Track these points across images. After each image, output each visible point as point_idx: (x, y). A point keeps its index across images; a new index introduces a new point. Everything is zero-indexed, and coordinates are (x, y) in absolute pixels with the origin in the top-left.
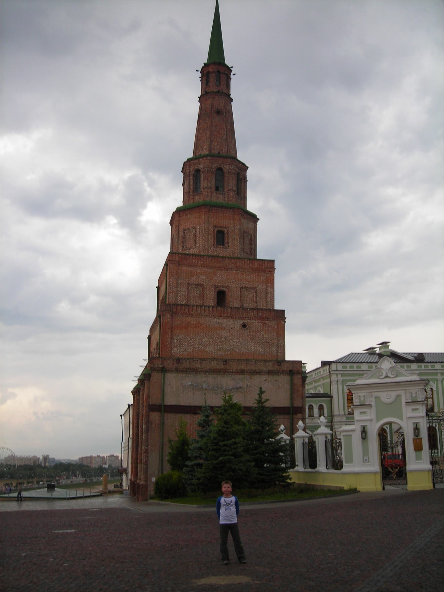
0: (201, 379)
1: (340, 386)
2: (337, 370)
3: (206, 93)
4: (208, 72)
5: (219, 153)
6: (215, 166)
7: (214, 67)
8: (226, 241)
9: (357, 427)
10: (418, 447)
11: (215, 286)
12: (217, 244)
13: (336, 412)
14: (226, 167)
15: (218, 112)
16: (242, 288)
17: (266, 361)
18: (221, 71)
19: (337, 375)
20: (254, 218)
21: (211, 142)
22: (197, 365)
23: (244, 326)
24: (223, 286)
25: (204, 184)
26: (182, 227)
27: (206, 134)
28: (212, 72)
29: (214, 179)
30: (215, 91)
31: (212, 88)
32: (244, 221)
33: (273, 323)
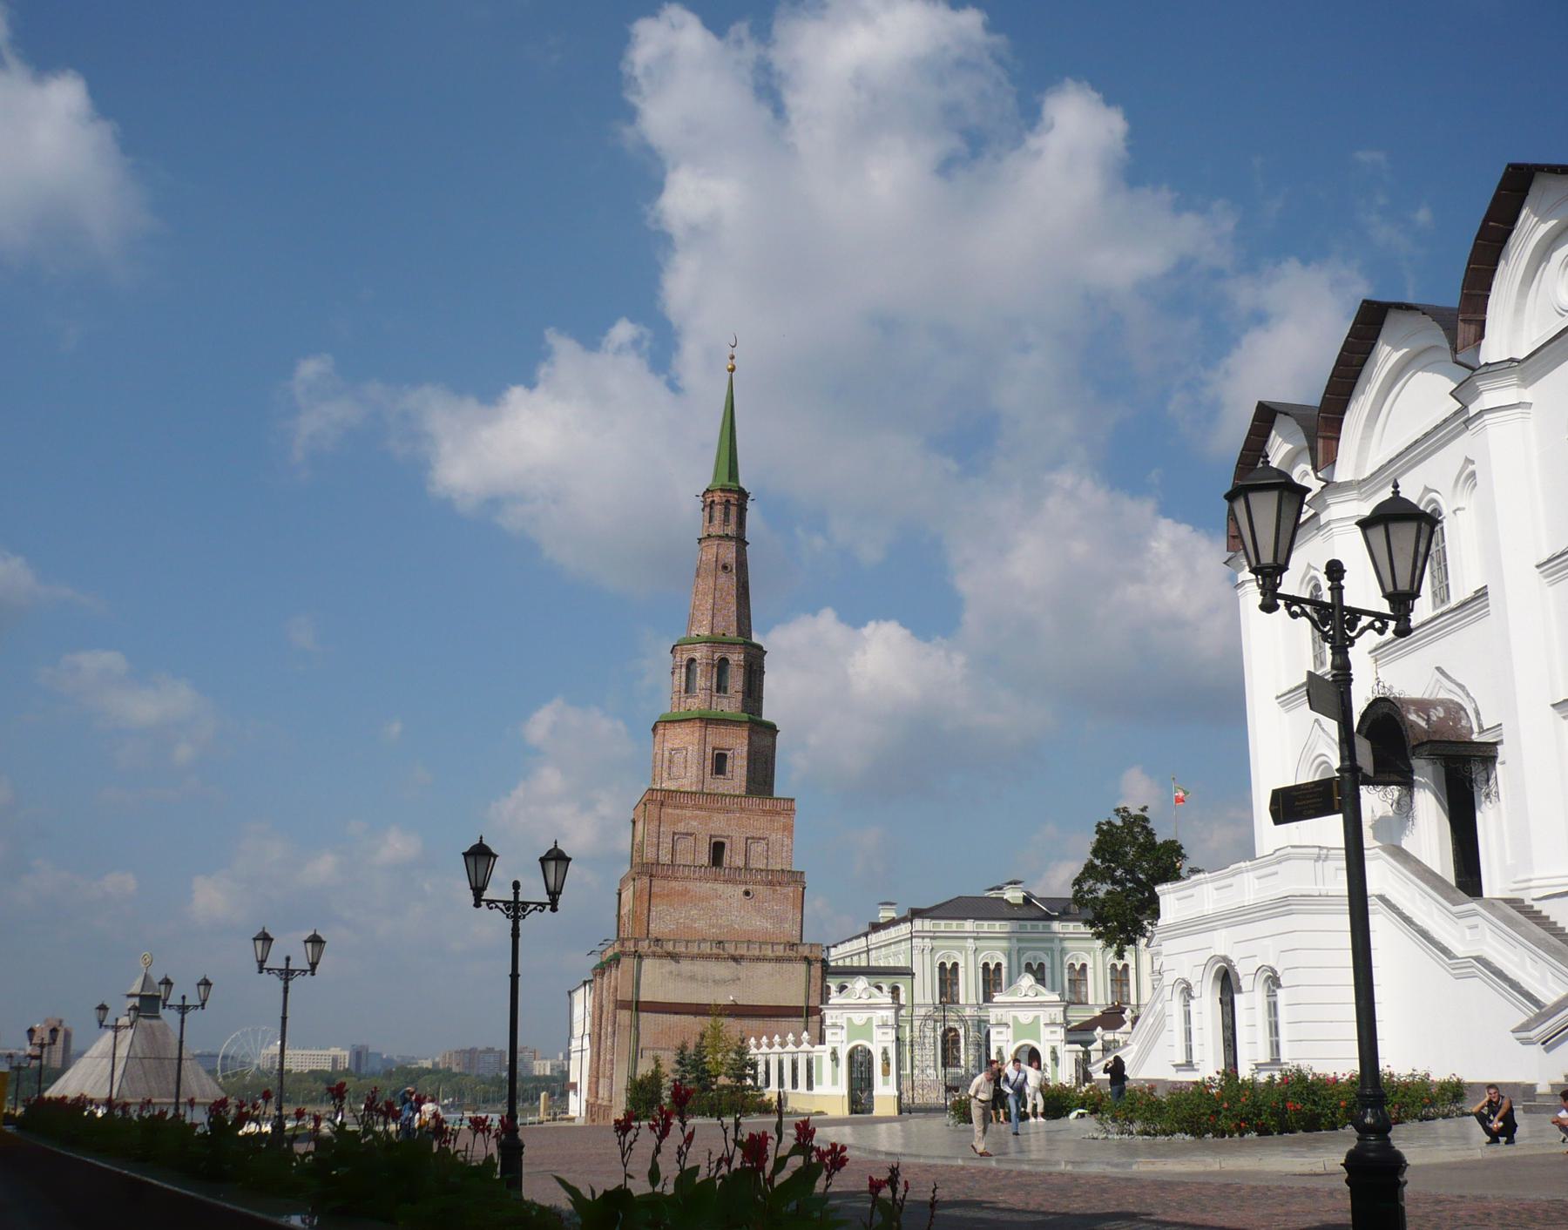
0: (686, 966)
1: (928, 957)
6: (716, 656)
9: (827, 1048)
10: (886, 1073)
13: (916, 1001)
15: (725, 567)
17: (773, 944)
18: (733, 501)
20: (772, 729)
22: (681, 949)
23: (747, 893)
25: (700, 682)
26: (668, 745)
31: (716, 529)
32: (754, 738)
33: (789, 890)
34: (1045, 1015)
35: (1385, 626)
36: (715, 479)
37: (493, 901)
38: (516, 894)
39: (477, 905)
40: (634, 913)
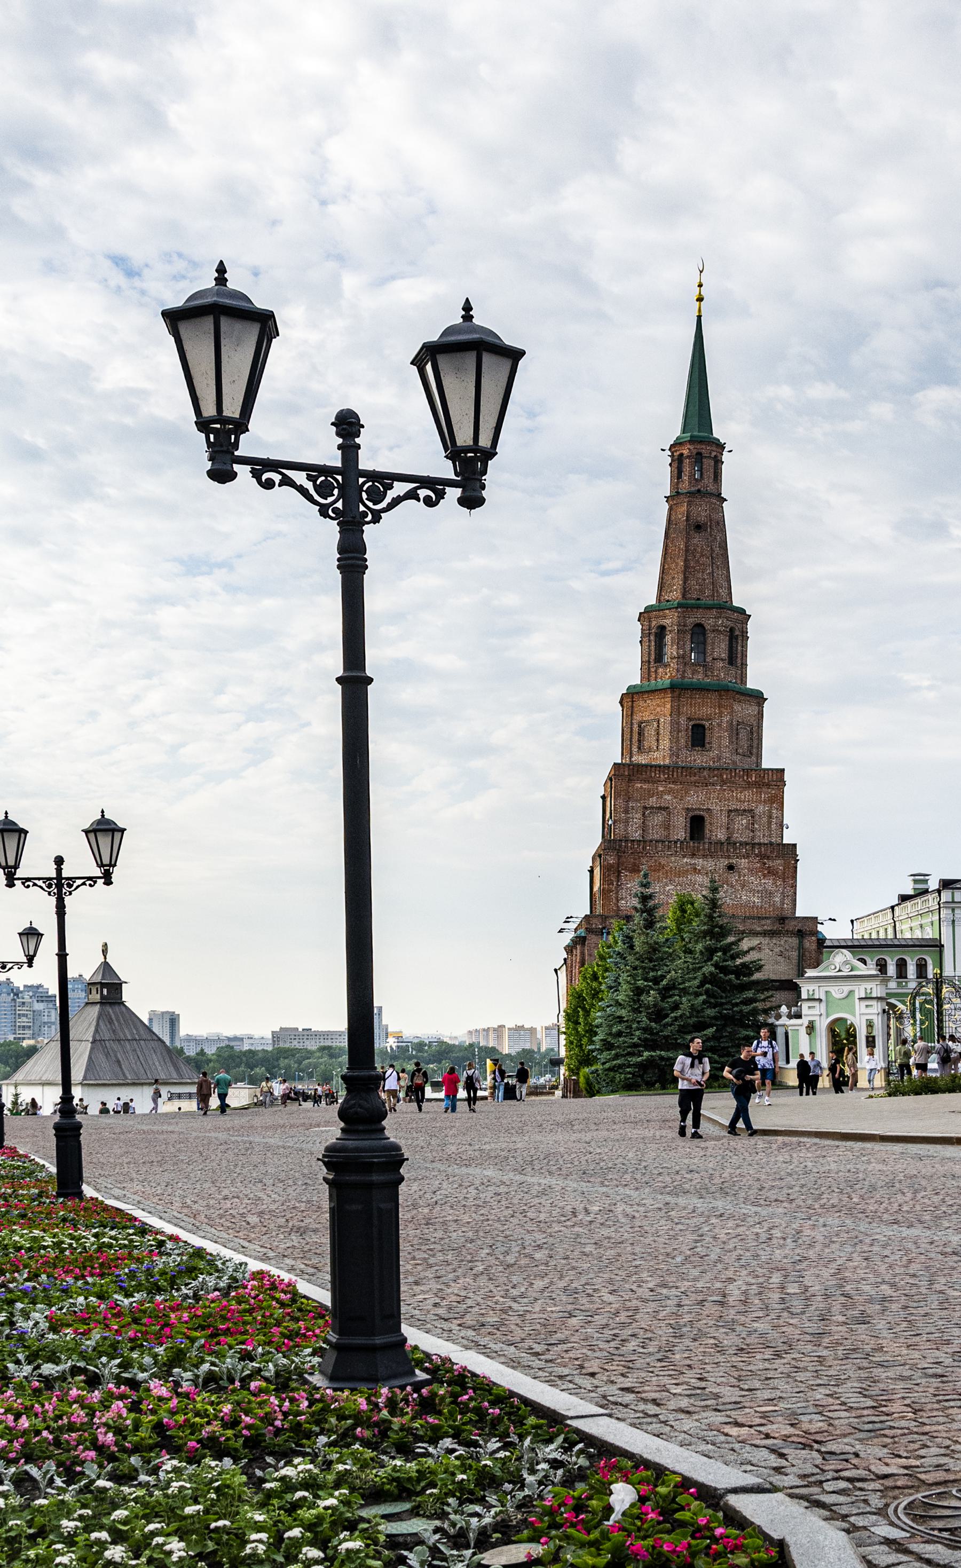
2: (953, 902)
3: (678, 493)
4: (682, 455)
5: (698, 599)
6: (691, 621)
7: (692, 448)
8: (707, 740)
11: (688, 809)
12: (693, 745)
14: (709, 623)
15: (699, 527)
16: (731, 811)
19: (953, 910)
21: (686, 579)
23: (731, 868)
24: (699, 809)
27: (677, 566)
28: (688, 457)
29: (688, 643)
30: (693, 489)
34: (860, 990)
35: (441, 495)
36: (684, 431)
37: (28, 879)
38: (59, 871)
39: (10, 884)
40: (605, 892)
